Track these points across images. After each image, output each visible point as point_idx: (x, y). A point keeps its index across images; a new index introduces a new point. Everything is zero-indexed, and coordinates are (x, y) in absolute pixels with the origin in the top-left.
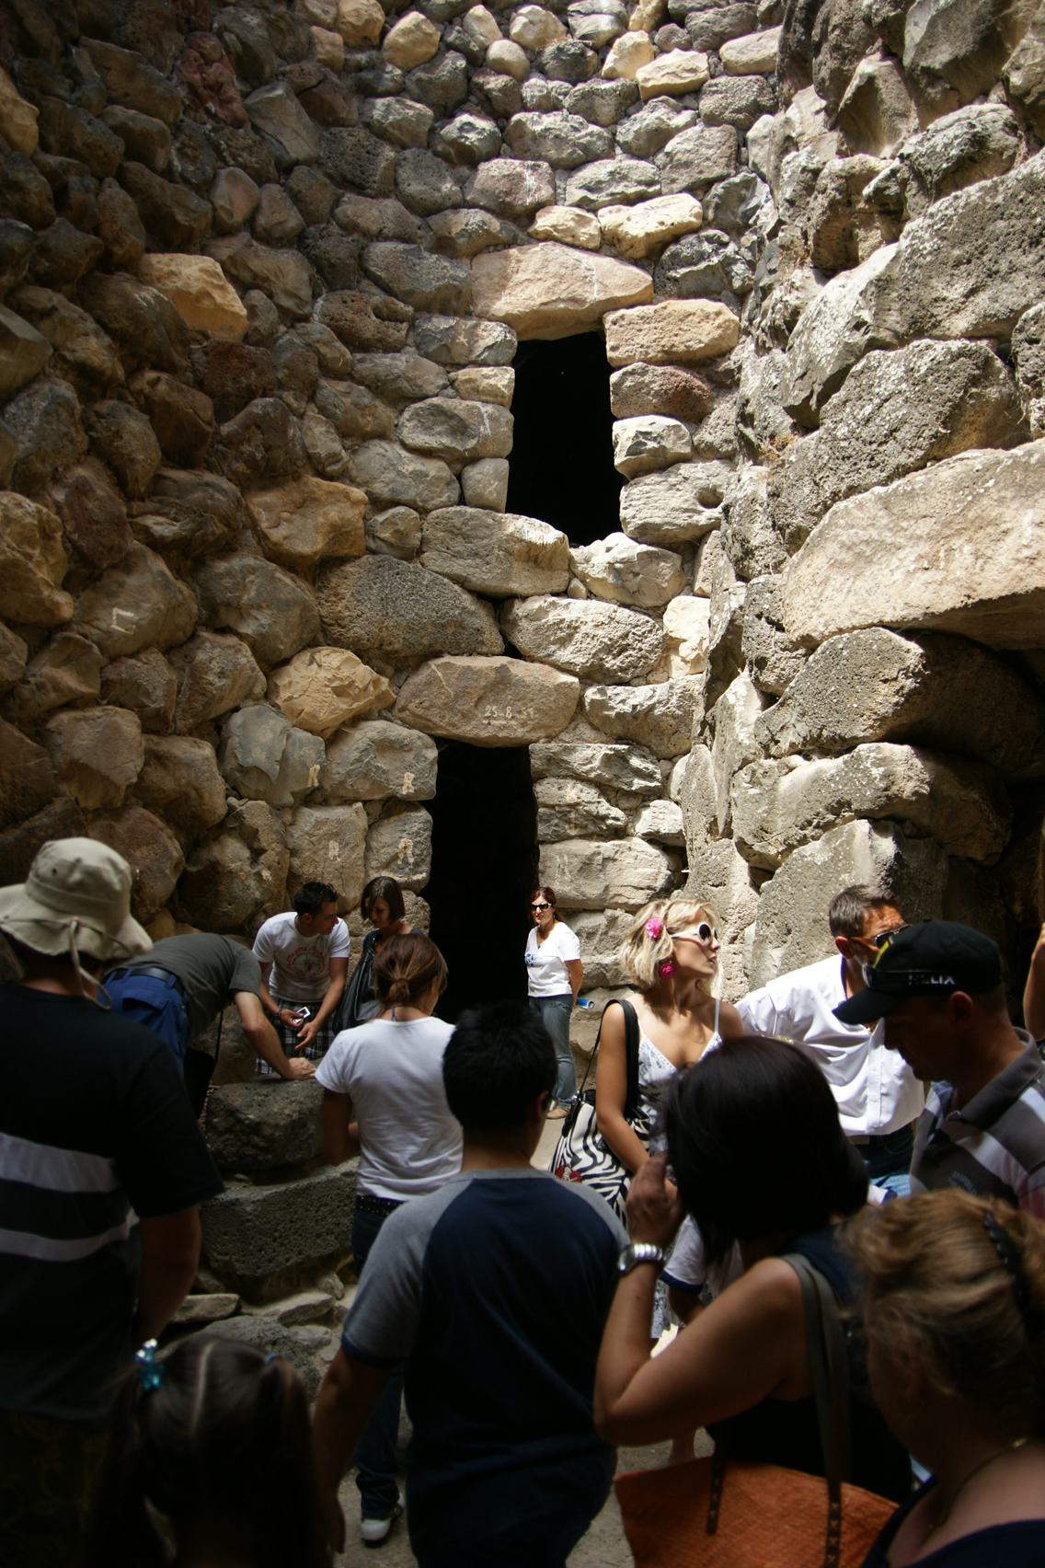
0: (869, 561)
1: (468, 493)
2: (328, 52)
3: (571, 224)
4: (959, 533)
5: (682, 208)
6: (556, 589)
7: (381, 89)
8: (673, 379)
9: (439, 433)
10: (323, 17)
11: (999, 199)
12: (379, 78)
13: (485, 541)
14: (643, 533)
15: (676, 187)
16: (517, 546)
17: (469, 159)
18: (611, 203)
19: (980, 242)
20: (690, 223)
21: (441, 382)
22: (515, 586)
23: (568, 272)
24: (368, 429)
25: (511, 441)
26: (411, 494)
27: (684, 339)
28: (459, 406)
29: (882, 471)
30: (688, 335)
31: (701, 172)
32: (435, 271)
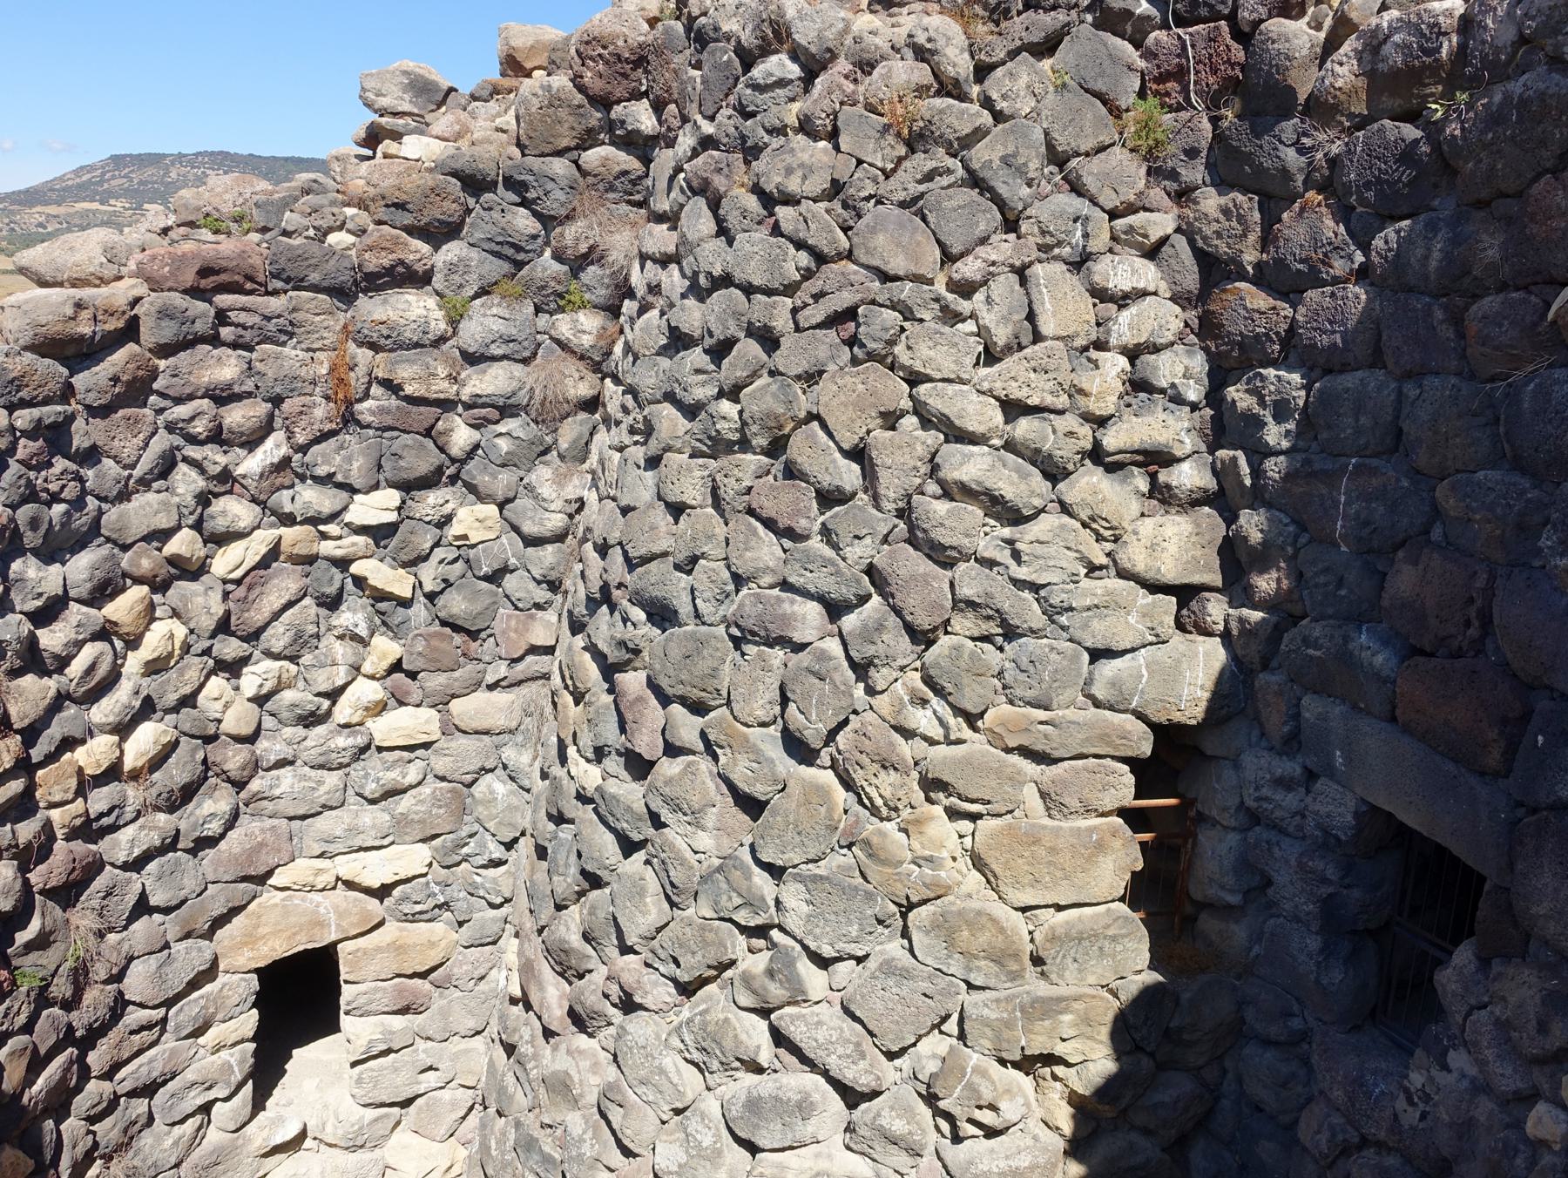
5: (411, 858)
15: (407, 838)
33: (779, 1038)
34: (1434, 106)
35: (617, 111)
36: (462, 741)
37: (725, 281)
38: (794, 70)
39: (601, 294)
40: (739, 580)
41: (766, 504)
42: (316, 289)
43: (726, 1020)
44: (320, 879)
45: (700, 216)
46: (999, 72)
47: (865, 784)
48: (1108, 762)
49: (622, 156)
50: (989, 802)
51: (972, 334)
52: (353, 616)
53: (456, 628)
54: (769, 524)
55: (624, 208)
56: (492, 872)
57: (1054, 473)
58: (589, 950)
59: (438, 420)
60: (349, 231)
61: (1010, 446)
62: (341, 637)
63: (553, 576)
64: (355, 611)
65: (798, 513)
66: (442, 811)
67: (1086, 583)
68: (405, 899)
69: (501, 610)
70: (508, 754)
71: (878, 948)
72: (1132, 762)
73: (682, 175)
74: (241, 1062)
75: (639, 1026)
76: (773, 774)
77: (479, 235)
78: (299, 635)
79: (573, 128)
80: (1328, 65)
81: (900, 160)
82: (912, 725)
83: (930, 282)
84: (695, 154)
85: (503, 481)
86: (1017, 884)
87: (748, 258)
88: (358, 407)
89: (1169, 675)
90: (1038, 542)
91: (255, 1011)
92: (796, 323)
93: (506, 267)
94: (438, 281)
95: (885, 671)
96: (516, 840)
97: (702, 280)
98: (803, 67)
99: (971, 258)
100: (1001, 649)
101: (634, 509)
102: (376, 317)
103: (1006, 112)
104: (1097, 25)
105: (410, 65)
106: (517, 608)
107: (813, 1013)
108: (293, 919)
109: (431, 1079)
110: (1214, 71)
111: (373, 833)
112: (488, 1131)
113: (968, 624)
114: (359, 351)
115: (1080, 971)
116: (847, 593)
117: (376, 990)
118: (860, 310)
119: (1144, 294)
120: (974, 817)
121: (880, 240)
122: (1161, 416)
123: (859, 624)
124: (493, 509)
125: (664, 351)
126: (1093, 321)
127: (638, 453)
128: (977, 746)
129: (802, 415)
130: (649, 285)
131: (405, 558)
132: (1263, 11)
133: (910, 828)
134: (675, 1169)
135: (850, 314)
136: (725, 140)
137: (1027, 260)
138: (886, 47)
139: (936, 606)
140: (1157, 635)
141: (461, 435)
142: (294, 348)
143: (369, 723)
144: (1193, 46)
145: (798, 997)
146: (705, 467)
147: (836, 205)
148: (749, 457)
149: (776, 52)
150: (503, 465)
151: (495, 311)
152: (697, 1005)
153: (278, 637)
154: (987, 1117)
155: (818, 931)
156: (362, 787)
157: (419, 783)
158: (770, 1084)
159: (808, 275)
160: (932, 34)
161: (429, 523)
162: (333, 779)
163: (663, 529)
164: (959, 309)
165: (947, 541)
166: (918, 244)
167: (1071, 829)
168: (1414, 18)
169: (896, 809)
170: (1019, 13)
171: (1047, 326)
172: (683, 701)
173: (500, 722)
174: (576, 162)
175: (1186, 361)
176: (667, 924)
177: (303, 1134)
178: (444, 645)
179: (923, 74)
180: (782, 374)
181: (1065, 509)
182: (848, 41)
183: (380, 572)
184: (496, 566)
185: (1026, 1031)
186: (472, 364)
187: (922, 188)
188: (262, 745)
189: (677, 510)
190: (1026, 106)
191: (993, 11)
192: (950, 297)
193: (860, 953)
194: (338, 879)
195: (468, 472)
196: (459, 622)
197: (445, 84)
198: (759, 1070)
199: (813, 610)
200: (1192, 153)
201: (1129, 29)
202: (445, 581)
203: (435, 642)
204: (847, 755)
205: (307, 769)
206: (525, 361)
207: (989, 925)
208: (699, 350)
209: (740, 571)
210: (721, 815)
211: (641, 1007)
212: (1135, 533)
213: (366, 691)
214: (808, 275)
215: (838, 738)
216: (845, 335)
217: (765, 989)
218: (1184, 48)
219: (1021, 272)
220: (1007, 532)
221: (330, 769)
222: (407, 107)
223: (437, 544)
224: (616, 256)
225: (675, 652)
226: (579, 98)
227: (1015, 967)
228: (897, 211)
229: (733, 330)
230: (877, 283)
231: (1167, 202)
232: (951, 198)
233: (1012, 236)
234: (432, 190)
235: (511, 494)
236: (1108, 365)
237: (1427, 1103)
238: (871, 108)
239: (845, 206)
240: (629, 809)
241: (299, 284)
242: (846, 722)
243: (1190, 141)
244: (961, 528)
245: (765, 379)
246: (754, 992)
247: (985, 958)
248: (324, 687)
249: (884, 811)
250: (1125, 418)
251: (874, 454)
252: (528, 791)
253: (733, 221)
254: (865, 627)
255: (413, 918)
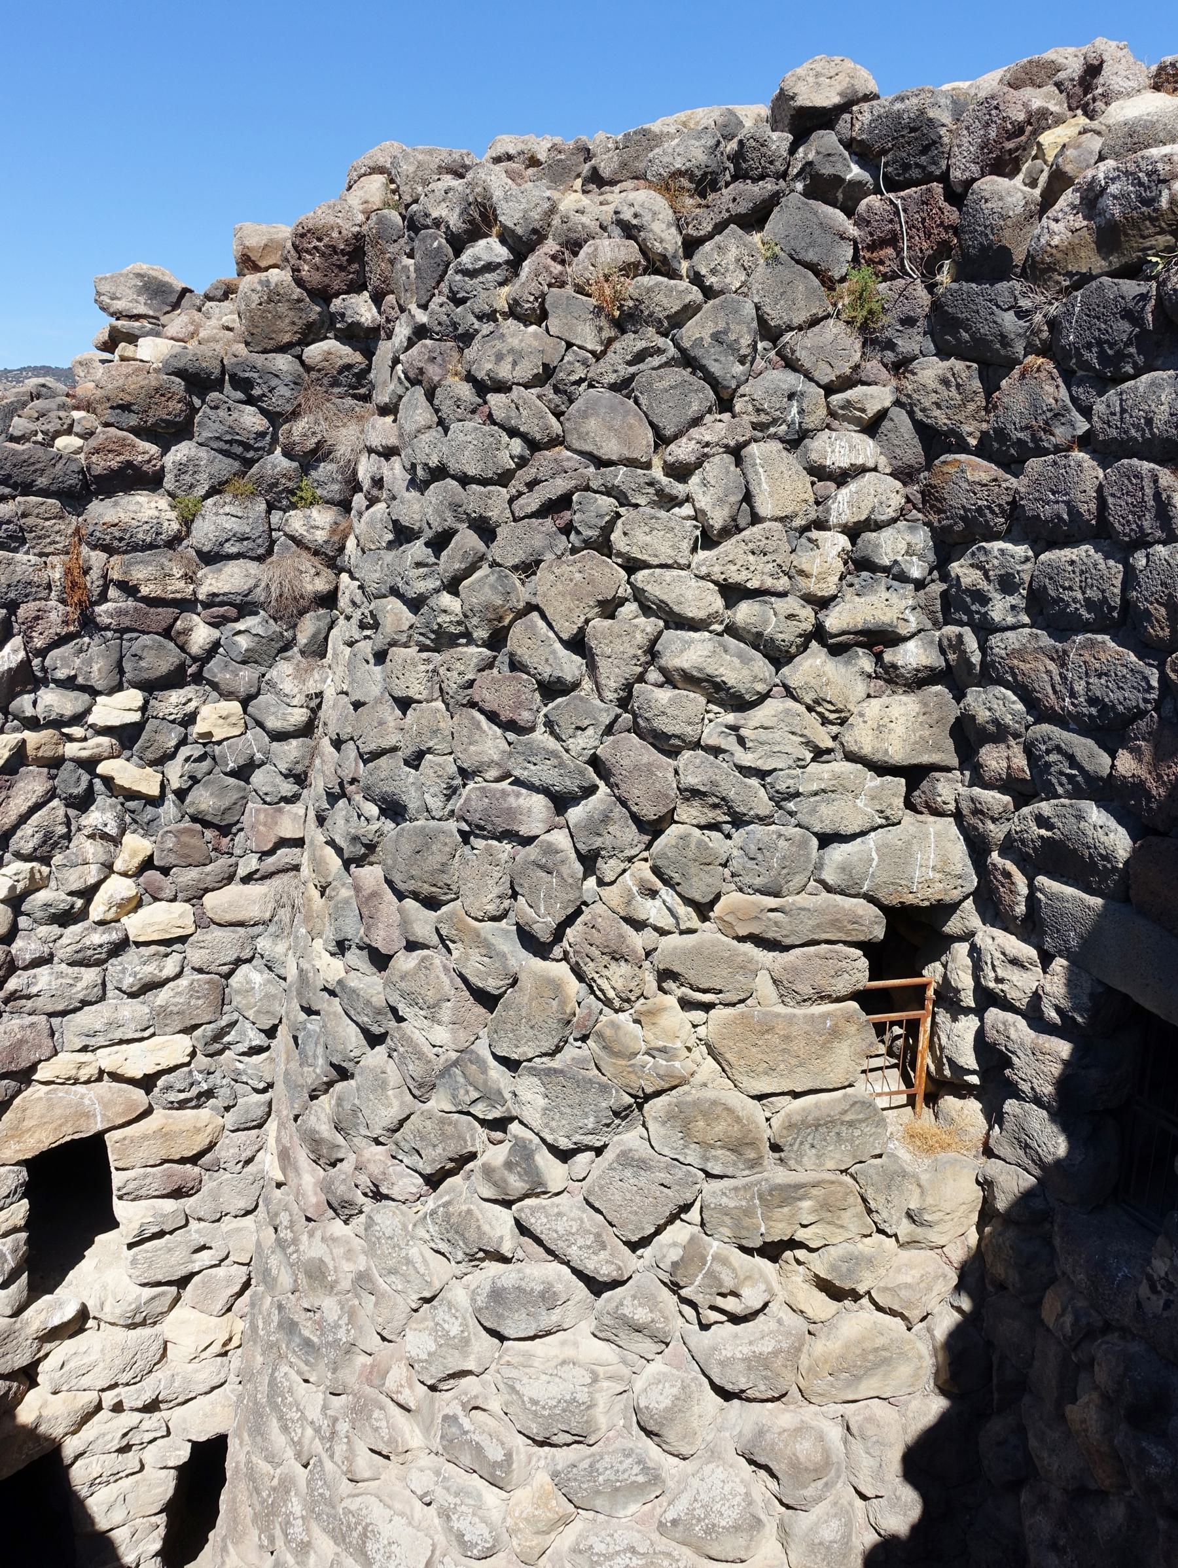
15: (167, 1029)
33: (523, 1229)
34: (1154, 259)
35: (337, 304)
36: (217, 933)
37: (439, 473)
38: (502, 253)
39: (334, 489)
40: (465, 774)
41: (488, 697)
42: (45, 493)
43: (469, 1212)
44: (82, 1072)
45: (416, 407)
46: (708, 246)
47: (596, 976)
48: (840, 947)
49: (347, 350)
50: (720, 992)
51: (688, 518)
52: (101, 816)
53: (206, 824)
54: (492, 717)
55: (349, 402)
56: (256, 1059)
57: (779, 657)
58: (339, 1139)
59: (176, 619)
60: (77, 435)
61: (732, 630)
62: (91, 836)
63: (299, 769)
64: (103, 811)
65: (519, 705)
66: (200, 1002)
67: (814, 767)
68: (168, 1088)
69: (250, 805)
70: (263, 944)
71: (616, 1138)
72: (867, 947)
73: (399, 367)
74: (15, 1251)
75: (386, 1217)
76: (505, 967)
77: (206, 434)
78: (48, 836)
79: (294, 323)
80: (1044, 219)
81: (610, 341)
82: (641, 916)
83: (648, 466)
84: (411, 343)
85: (246, 676)
86: (752, 1072)
87: (461, 448)
88: (98, 609)
89: (900, 857)
90: (762, 727)
91: (26, 1201)
92: (513, 513)
93: (237, 465)
94: (169, 482)
95: (612, 862)
96: (275, 1028)
97: (420, 472)
98: (511, 249)
99: (684, 440)
100: (728, 836)
101: (364, 704)
102: (107, 519)
103: (716, 287)
104: (808, 193)
105: (144, 268)
106: (265, 802)
107: (553, 1205)
108: (58, 1112)
109: (205, 1258)
110: (928, 235)
111: (133, 1026)
112: (256, 1311)
113: (694, 812)
114: (93, 554)
115: (818, 1157)
116: (571, 785)
117: (146, 1176)
118: (575, 498)
119: (863, 470)
120: (707, 1007)
121: (592, 424)
122: (885, 595)
123: (584, 815)
124: (235, 707)
125: (391, 545)
126: (812, 500)
127: (366, 648)
128: (707, 936)
129: (521, 605)
130: (373, 479)
131: (150, 755)
132: (975, 168)
133: (642, 1018)
134: (425, 1357)
135: (563, 503)
136: (438, 328)
137: (742, 439)
138: (594, 226)
139: (661, 795)
140: (887, 818)
141: (201, 635)
142: (27, 553)
143: (124, 920)
144: (905, 210)
145: (536, 1190)
146: (428, 661)
147: (548, 390)
148: (473, 649)
149: (486, 236)
150: (244, 662)
151: (227, 509)
152: (441, 1197)
153: (26, 839)
154: (730, 1304)
155: (554, 1124)
156: (120, 981)
157: (178, 975)
158: (513, 1275)
159: (522, 462)
160: (637, 209)
161: (173, 722)
162: (90, 975)
163: (392, 724)
164: (674, 492)
165: (669, 729)
166: (631, 427)
167: (805, 1016)
168: (1132, 167)
169: (628, 1001)
170: (727, 185)
171: (765, 507)
172: (416, 896)
173: (253, 912)
174: (299, 357)
175: (909, 538)
176: (408, 1117)
177: (83, 1314)
178: (195, 841)
179: (629, 251)
180: (500, 565)
181: (790, 693)
182: (556, 221)
183: (125, 772)
184: (241, 762)
185: (766, 1218)
186: (207, 564)
187: (632, 370)
188: (18, 944)
189: (404, 704)
190: (735, 280)
191: (699, 183)
192: (665, 480)
193: (598, 1144)
194: (101, 1072)
195: (209, 670)
196: (208, 818)
197: (179, 285)
198: (505, 1260)
199: (539, 802)
200: (908, 321)
201: (840, 196)
202: (191, 777)
203: (185, 839)
204: (577, 948)
205: (64, 965)
206: (260, 559)
207: (725, 1114)
208: (421, 541)
209: (465, 766)
210: (455, 1009)
211: (387, 1197)
212: (861, 715)
213: (118, 888)
214: (522, 462)
215: (568, 930)
216: (561, 523)
217: (505, 1181)
218: (897, 213)
219: (736, 452)
220: (731, 718)
221: (88, 966)
222: (141, 309)
223: (183, 742)
224: (343, 450)
225: (407, 848)
226: (298, 292)
227: (752, 1155)
228: (608, 394)
229: (450, 522)
230: (592, 469)
231: (884, 374)
232: (661, 378)
233: (726, 416)
234: (157, 390)
235: (253, 690)
236: (828, 544)
237: (1170, 1291)
238: (580, 290)
239: (557, 390)
240: (368, 1003)
241: (27, 489)
242: (578, 913)
243: (906, 309)
244: (683, 716)
245: (484, 570)
246: (495, 1184)
247: (722, 1147)
248: (76, 886)
249: (617, 1003)
250: (847, 598)
251: (593, 644)
252: (285, 979)
253: (447, 409)
254: (590, 818)
255: (182, 1105)
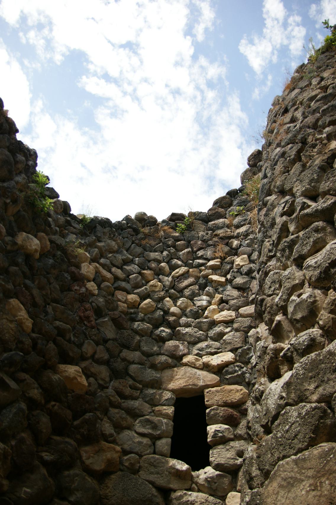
0: (292, 486)
1: (157, 450)
2: (122, 309)
3: (194, 361)
4: (323, 476)
5: (228, 356)
6: (187, 488)
7: (137, 319)
8: (227, 412)
9: (148, 428)
10: (122, 300)
11: (321, 358)
12: (137, 317)
13: (162, 468)
14: (217, 467)
15: (226, 350)
16: (173, 471)
17: (162, 340)
18: (206, 355)
19: (317, 371)
20: (231, 361)
21: (150, 411)
22: (171, 486)
23: (193, 376)
24: (124, 426)
25: (172, 432)
26: (137, 450)
27: (230, 398)
28: (156, 419)
29: (294, 450)
30: (232, 397)
31: (234, 346)
32: (150, 374)
153: (187, 292)
